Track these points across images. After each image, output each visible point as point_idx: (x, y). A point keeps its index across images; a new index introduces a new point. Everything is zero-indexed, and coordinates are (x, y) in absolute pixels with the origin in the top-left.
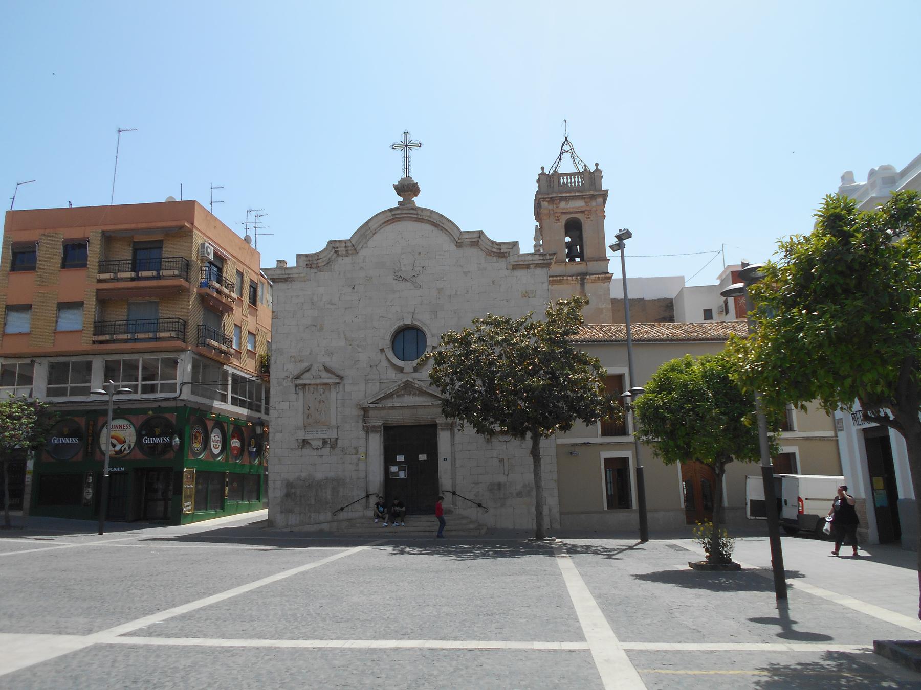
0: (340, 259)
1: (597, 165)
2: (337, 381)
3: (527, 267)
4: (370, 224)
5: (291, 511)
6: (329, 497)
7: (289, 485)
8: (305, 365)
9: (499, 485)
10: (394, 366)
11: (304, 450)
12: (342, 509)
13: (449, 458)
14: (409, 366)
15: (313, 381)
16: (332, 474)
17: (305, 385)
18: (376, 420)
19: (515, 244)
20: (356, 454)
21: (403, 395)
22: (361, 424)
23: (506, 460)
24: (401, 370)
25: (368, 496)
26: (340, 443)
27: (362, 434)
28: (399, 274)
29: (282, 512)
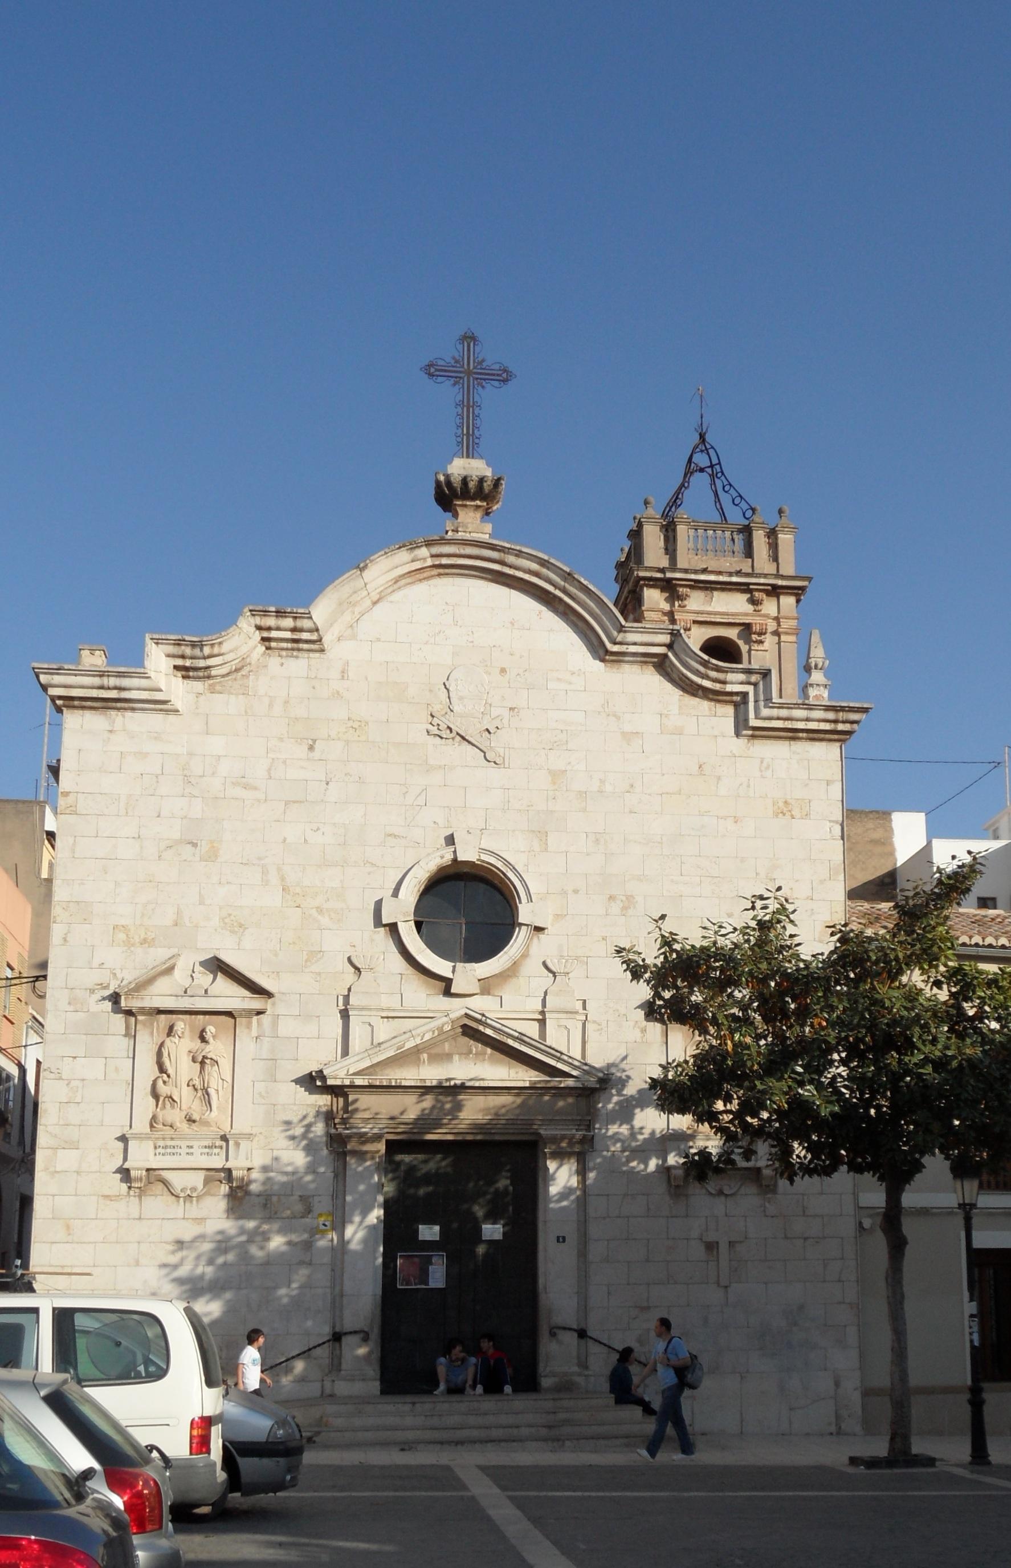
8: (158, 955)
14: (467, 975)
25: (337, 1337)
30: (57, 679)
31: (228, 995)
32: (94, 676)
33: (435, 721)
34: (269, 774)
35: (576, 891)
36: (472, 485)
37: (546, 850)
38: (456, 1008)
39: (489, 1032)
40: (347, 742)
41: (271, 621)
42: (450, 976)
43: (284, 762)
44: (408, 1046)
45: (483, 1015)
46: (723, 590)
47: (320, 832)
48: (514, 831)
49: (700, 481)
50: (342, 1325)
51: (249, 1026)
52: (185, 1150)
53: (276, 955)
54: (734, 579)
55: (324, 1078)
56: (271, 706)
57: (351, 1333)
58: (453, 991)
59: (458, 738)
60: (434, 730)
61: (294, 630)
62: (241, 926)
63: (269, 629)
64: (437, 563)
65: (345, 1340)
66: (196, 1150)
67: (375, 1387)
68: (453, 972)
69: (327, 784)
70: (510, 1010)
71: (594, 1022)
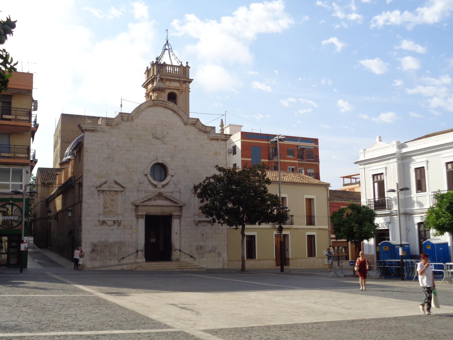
0: (123, 123)
1: (187, 63)
2: (122, 190)
3: (218, 140)
4: (141, 107)
5: (95, 259)
6: (117, 252)
7: (94, 245)
8: (103, 180)
9: (201, 247)
10: (152, 184)
11: (103, 226)
12: (123, 258)
14: (160, 184)
15: (109, 189)
17: (103, 191)
18: (143, 212)
19: (214, 128)
22: (134, 213)
24: (156, 186)
25: (137, 251)
27: (135, 219)
29: (90, 260)
30: (84, 126)
49: (167, 52)
54: (176, 79)
61: (128, 117)
65: (139, 252)
67: (144, 260)
70: (166, 191)
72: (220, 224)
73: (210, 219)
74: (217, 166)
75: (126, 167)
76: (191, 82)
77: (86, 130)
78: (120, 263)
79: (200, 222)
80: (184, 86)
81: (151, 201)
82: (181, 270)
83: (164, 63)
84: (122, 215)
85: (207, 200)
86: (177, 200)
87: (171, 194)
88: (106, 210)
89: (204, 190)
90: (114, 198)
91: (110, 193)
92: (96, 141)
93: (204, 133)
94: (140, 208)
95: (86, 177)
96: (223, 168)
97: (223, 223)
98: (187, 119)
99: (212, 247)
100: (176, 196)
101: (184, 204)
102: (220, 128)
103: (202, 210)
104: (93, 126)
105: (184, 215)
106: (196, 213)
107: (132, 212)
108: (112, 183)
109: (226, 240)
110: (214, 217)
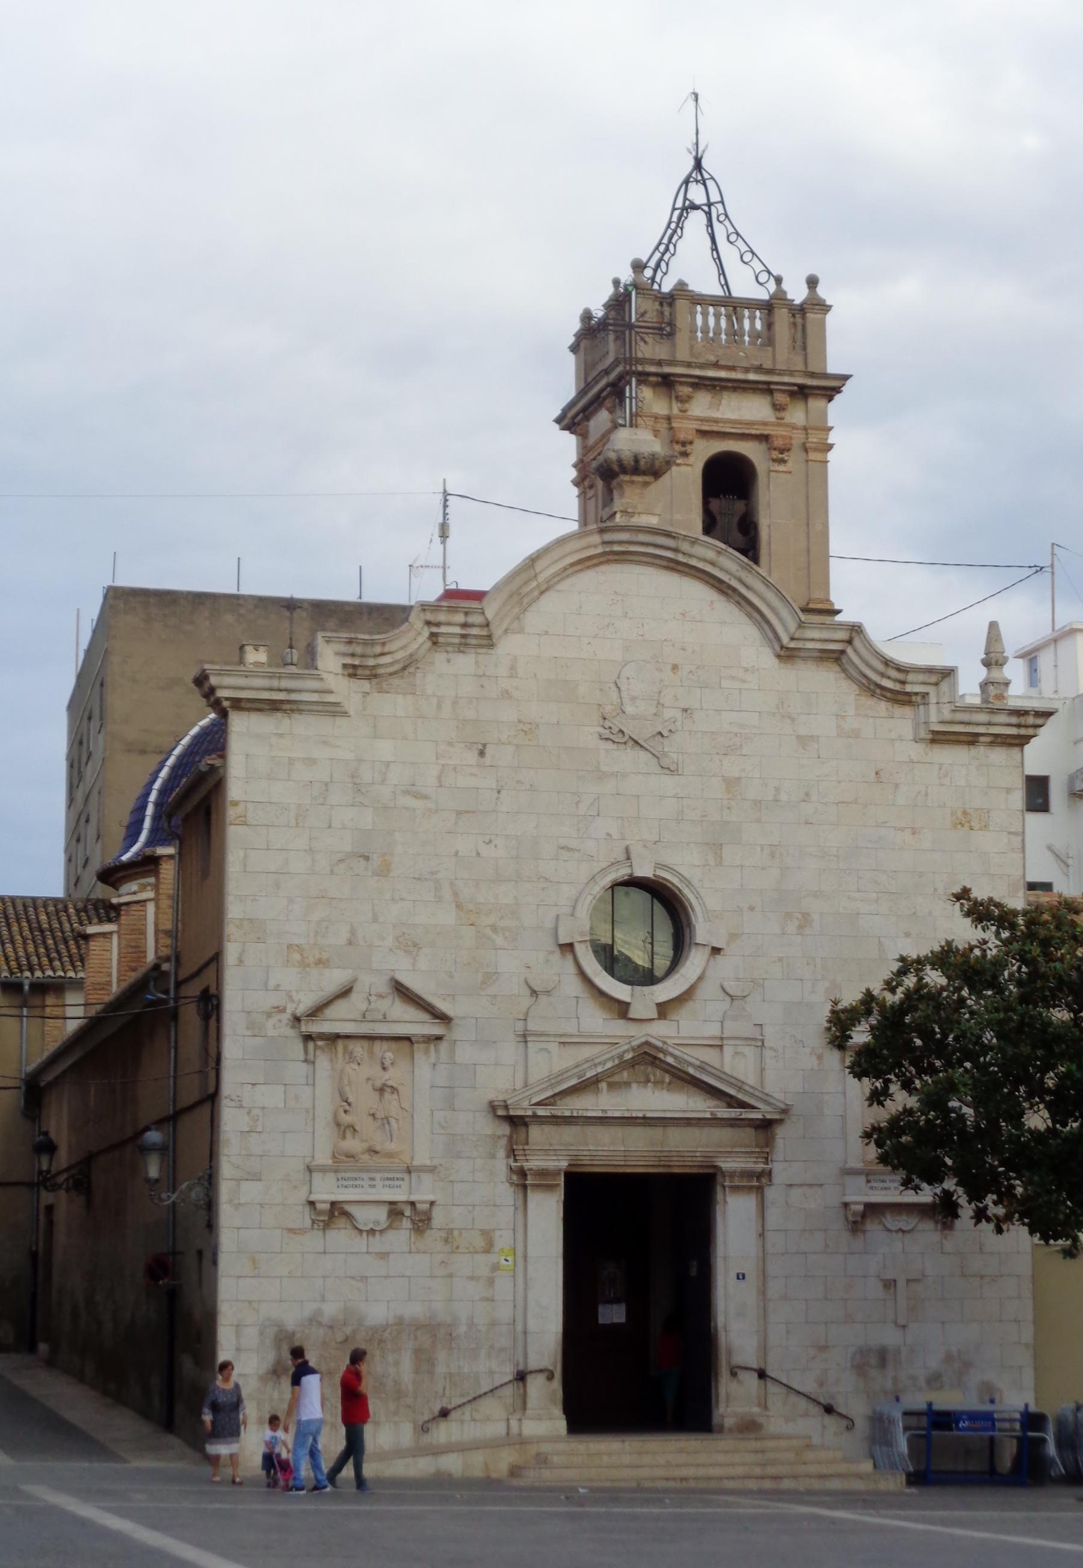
0: (439, 657)
1: (812, 282)
2: (436, 1030)
3: (972, 740)
4: (540, 565)
8: (334, 979)
9: (883, 1356)
10: (601, 994)
11: (331, 1234)
12: (444, 1414)
13: (752, 1276)
14: (644, 1000)
16: (414, 1310)
18: (553, 1151)
19: (947, 674)
20: (488, 1249)
21: (627, 1084)
22: (501, 1164)
23: (901, 1284)
24: (621, 1009)
25: (521, 1377)
26: (438, 1217)
27: (506, 1193)
28: (618, 723)
31: (408, 1021)
32: (264, 677)
33: (607, 724)
34: (440, 781)
35: (752, 909)
36: (642, 463)
37: (721, 864)
38: (638, 1034)
39: (670, 1060)
40: (517, 746)
41: (442, 617)
42: (627, 999)
43: (455, 769)
44: (589, 1075)
45: (665, 1043)
46: (735, 389)
47: (492, 845)
48: (688, 844)
49: (696, 221)
50: (526, 1363)
51: (427, 1052)
52: (366, 1183)
53: (451, 977)
54: (752, 377)
55: (506, 1107)
56: (439, 707)
57: (536, 1371)
58: (631, 1015)
59: (631, 743)
60: (606, 733)
61: (465, 625)
62: (415, 945)
63: (438, 624)
64: (608, 550)
65: (530, 1379)
66: (378, 1183)
67: (562, 1425)
68: (632, 996)
69: (499, 792)
70: (683, 1035)
71: (771, 1048)
72: (987, 1227)
73: (927, 1195)
74: (963, 895)
75: (459, 906)
76: (837, 390)
77: (238, 704)
78: (426, 1439)
79: (873, 1210)
80: (796, 415)
81: (598, 1091)
82: (768, 1484)
83: (681, 286)
84: (432, 1170)
85: (907, 1086)
86: (740, 1086)
87: (709, 1056)
88: (352, 1144)
89: (890, 1036)
90: (393, 1076)
91: (371, 1053)
92: (291, 761)
93: (896, 701)
94: (536, 1133)
95: (241, 961)
96: (998, 905)
97: (1008, 1217)
98: (792, 625)
99: (949, 1359)
100: (738, 1066)
101: (784, 1111)
102: (982, 673)
103: (879, 1144)
104: (275, 683)
105: (781, 1172)
106: (855, 1163)
107: (493, 1156)
108: (381, 996)
109: (1030, 1316)
110: (950, 1184)
